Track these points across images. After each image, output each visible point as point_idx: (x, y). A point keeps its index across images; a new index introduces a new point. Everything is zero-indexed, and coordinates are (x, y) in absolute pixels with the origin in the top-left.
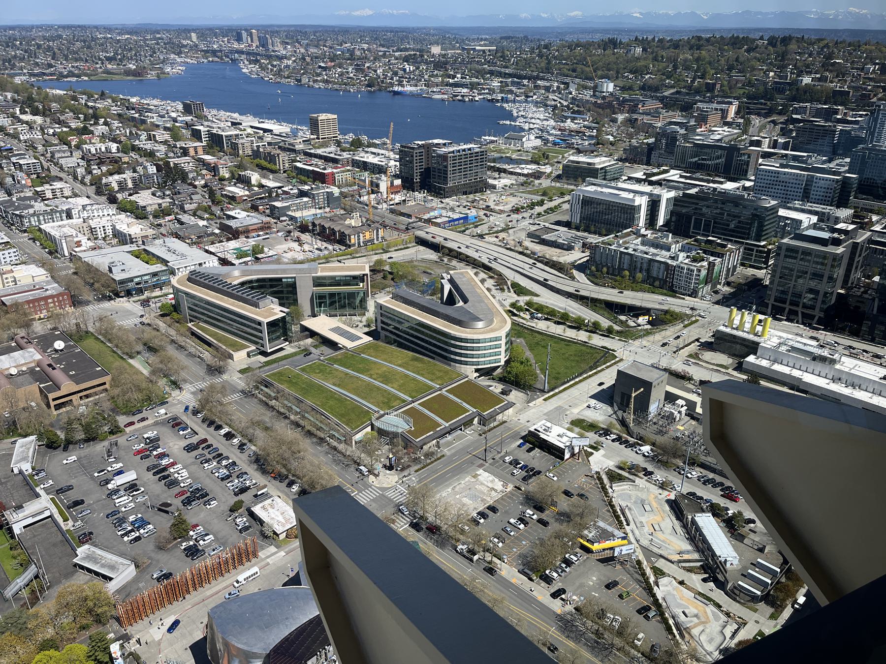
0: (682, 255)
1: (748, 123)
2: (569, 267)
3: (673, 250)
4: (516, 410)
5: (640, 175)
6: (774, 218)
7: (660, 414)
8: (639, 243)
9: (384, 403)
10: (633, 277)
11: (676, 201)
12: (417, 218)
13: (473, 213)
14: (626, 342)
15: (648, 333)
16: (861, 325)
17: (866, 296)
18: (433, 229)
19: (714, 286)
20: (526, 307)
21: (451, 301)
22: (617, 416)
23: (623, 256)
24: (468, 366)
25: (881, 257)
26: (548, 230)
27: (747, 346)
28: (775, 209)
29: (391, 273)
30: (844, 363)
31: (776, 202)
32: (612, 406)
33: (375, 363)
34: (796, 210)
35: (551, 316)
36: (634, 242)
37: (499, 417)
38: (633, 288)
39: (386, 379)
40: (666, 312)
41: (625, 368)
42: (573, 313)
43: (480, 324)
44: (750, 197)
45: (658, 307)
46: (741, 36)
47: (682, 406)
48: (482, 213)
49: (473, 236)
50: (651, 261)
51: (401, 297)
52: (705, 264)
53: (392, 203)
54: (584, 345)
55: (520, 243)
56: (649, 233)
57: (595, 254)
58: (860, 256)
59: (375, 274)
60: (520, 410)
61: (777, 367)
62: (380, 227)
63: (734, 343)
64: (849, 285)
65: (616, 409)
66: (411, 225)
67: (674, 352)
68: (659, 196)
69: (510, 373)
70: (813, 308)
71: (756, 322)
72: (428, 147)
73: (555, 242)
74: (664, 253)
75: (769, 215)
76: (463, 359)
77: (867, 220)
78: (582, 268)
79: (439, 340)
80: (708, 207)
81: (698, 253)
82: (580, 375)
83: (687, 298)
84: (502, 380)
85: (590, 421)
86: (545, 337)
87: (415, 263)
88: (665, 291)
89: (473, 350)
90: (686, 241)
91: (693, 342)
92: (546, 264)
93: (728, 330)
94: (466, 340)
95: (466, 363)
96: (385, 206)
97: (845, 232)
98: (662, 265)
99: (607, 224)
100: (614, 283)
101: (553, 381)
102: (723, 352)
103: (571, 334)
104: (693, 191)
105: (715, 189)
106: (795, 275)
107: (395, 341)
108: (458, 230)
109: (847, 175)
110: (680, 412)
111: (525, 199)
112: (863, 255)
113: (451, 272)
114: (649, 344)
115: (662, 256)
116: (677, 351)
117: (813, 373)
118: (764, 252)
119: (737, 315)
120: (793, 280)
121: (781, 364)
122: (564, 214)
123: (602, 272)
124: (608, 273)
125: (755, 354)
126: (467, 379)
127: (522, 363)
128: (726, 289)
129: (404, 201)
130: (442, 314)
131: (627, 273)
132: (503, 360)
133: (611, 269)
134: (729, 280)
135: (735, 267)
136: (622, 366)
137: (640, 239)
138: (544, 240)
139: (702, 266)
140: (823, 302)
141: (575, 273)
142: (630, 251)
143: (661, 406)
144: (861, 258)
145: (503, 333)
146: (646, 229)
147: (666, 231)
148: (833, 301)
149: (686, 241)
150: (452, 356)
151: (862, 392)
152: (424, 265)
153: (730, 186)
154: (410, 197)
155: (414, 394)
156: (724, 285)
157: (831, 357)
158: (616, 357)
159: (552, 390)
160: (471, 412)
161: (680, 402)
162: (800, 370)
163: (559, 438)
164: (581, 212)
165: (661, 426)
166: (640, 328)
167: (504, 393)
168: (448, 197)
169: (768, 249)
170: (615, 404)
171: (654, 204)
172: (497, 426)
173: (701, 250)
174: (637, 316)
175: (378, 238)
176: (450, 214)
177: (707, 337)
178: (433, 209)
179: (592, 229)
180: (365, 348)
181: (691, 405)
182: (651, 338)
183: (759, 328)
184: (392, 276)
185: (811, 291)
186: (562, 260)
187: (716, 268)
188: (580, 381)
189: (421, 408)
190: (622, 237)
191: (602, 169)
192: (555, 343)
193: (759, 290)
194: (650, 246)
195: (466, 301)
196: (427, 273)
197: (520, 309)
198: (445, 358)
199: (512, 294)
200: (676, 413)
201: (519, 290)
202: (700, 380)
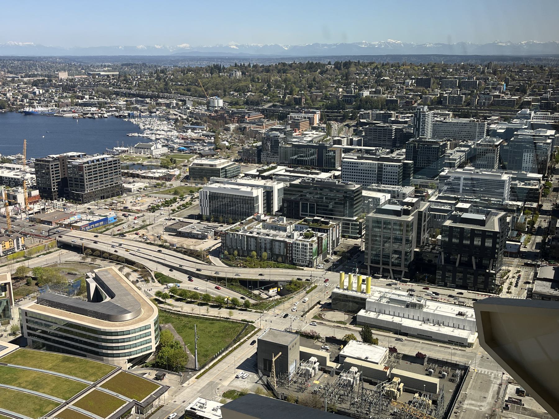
0: (296, 234)
1: (329, 127)
2: (205, 253)
3: (288, 230)
4: (171, 393)
5: (254, 172)
6: (359, 198)
7: (298, 373)
8: (261, 227)
9: (35, 411)
10: (260, 256)
11: (285, 191)
12: (57, 224)
13: (111, 214)
14: (261, 313)
15: (278, 303)
16: (435, 274)
17: (434, 251)
18: (74, 233)
19: (325, 256)
20: (170, 294)
21: (98, 298)
22: (263, 382)
23: (249, 239)
24: (121, 358)
25: (440, 220)
26: (183, 224)
27: (357, 303)
28: (358, 191)
29: (34, 279)
30: (429, 306)
31: (359, 186)
32: (257, 373)
33: (23, 370)
34: (374, 190)
35: (194, 299)
36: (257, 227)
37: (156, 403)
38: (261, 265)
39: (36, 385)
40: (291, 282)
41: (264, 336)
42: (213, 294)
43: (128, 316)
44: (340, 183)
45: (283, 279)
46: (315, 62)
47: (315, 363)
48: (120, 214)
49: (114, 235)
50: (273, 240)
51: (46, 300)
52: (315, 239)
53: (30, 212)
54: (226, 321)
55: (159, 237)
56: (267, 218)
57: (225, 240)
58: (425, 221)
59: (18, 282)
60: (176, 392)
61: (382, 317)
62: (20, 236)
63: (347, 301)
64: (421, 244)
65: (261, 375)
66: (52, 231)
67: (302, 316)
68: (271, 188)
69: (161, 358)
70: (399, 265)
71: (361, 281)
72: (63, 160)
73: (191, 233)
74: (282, 233)
75: (356, 196)
76: (115, 352)
77: (425, 194)
78: (216, 253)
79: (89, 337)
80: (310, 193)
81: (308, 231)
82: (226, 349)
83: (305, 268)
84: (155, 366)
85: (240, 390)
86: (191, 319)
87: (59, 266)
88: (287, 265)
89: (124, 342)
90: (298, 222)
91: (316, 305)
92: (185, 253)
93: (341, 291)
94: (116, 334)
95: (118, 356)
96: (24, 215)
97: (412, 204)
98: (282, 244)
99: (233, 214)
100: (245, 263)
101: (203, 359)
102: (340, 310)
103: (214, 312)
105: (313, 179)
106: (382, 241)
107: (44, 345)
108: (99, 231)
110: (314, 368)
111: (159, 198)
112: (427, 220)
113: (96, 271)
114: (281, 312)
115: (281, 236)
116: (304, 315)
117: (408, 318)
118: (357, 225)
119: (345, 278)
120: (382, 245)
121: (385, 314)
122: (195, 209)
123: (234, 255)
124: (239, 255)
125: (364, 308)
126: (120, 371)
127: (172, 346)
128: (334, 258)
129: (43, 209)
130: (90, 311)
131: (254, 253)
132: (154, 346)
133: (241, 252)
134: (335, 250)
135: (338, 239)
136: (260, 336)
137: (261, 224)
138: (180, 232)
139: (313, 241)
140: (406, 260)
141: (211, 258)
142: (254, 234)
143: (298, 365)
144: (426, 223)
145: (151, 321)
147: (281, 215)
148: (412, 259)
149: (298, 222)
150: (104, 351)
151: (446, 328)
152: (68, 267)
153: (324, 176)
154: (49, 205)
155: (67, 395)
156: (332, 254)
157: (419, 302)
158: (255, 328)
159: (203, 367)
160: (128, 403)
161: (313, 359)
162: (399, 316)
163: (214, 412)
164: (210, 206)
165: (301, 384)
166: (271, 299)
167: (158, 378)
168: (86, 203)
169: (360, 222)
170: (259, 371)
171: (268, 194)
172: (155, 412)
173: (310, 228)
174: (267, 289)
175: (18, 246)
176: (90, 217)
177: (325, 300)
178: (73, 214)
179: (221, 219)
180: (12, 357)
181: (322, 360)
182: (281, 306)
183: (364, 287)
184: (36, 282)
185: (396, 252)
186: (198, 248)
187: (324, 241)
188: (227, 355)
189: (76, 408)
190: (246, 224)
191: (222, 169)
192: (201, 323)
193: (358, 256)
194: (270, 229)
195: (112, 295)
196: (72, 274)
197: (165, 296)
198: (97, 353)
199: (157, 284)
200: (311, 370)
201: (162, 278)
202: (326, 338)
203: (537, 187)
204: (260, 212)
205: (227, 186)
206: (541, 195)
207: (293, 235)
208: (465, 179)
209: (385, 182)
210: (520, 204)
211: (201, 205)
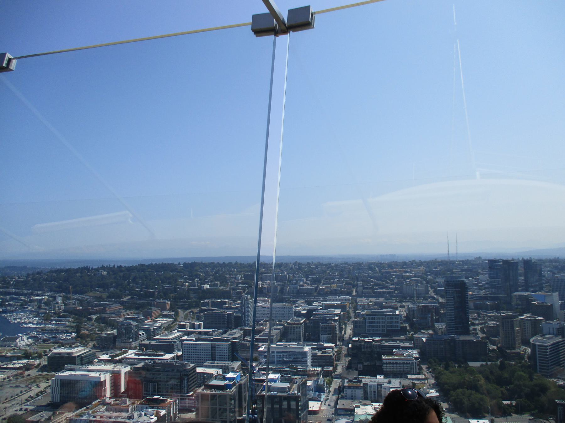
1: (177, 314)
3: (130, 411)
5: (107, 357)
28: (194, 368)
31: (193, 365)
56: (112, 401)
97: (233, 379)
104: (141, 365)
109: (234, 341)
137: (105, 407)
142: (98, 418)
146: (110, 398)
149: (139, 402)
153: (168, 356)
164: (61, 393)
191: (78, 356)
203: (331, 354)
204: (107, 395)
205: (78, 373)
206: (334, 360)
207: (133, 415)
208: (277, 352)
209: (218, 359)
210: (319, 369)
211: (52, 393)
